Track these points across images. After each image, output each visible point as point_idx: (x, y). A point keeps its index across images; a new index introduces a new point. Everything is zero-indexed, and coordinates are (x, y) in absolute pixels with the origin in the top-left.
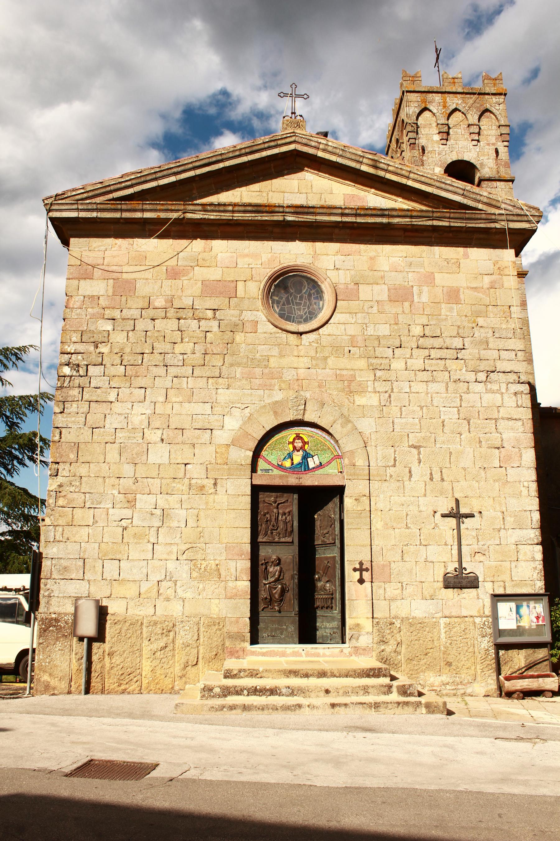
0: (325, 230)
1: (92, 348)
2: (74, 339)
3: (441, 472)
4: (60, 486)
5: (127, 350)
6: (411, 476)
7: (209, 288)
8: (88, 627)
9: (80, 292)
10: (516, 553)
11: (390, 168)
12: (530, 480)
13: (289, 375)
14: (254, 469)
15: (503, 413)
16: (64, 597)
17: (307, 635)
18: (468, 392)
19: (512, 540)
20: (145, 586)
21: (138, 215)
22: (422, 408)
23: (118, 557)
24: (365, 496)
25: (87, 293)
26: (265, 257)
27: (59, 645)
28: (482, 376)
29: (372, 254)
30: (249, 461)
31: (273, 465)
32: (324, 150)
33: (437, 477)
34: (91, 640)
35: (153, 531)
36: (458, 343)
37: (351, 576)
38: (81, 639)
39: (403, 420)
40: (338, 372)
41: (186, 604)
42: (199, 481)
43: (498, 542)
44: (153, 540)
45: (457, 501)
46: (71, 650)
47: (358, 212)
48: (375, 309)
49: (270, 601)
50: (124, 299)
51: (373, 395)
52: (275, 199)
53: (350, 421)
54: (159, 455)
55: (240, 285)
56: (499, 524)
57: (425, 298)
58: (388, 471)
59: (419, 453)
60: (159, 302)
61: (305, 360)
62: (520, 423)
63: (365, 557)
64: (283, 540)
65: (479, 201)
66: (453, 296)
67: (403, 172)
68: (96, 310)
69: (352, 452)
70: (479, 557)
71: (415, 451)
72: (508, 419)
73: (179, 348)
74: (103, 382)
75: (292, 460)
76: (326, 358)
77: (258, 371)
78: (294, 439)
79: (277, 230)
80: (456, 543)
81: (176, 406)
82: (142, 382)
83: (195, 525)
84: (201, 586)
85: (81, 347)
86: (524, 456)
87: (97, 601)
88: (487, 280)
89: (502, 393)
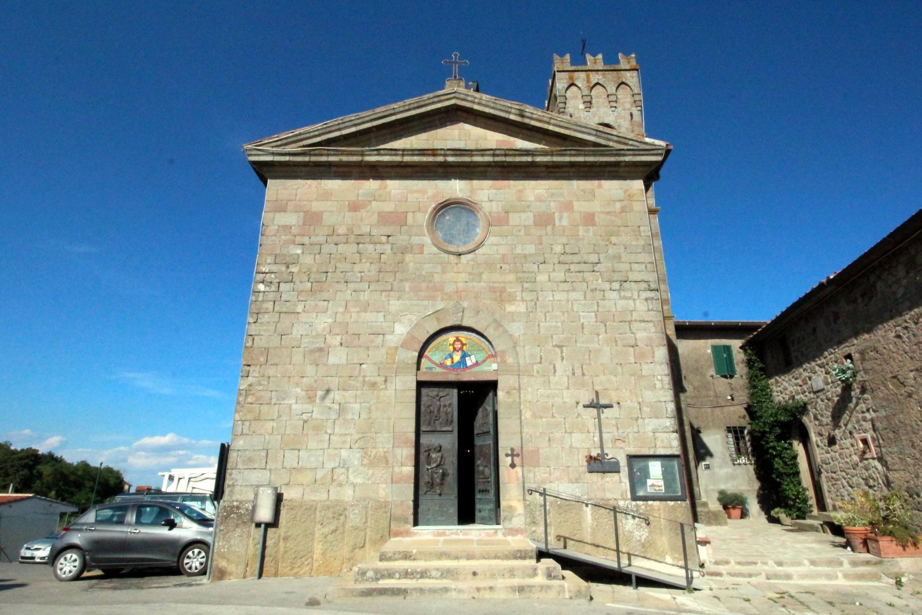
0: (479, 169)
1: (284, 268)
2: (269, 261)
4: (250, 385)
5: (315, 269)
6: (555, 371)
7: (384, 218)
8: (265, 514)
9: (275, 222)
11: (534, 116)
13: (450, 288)
14: (418, 369)
15: (635, 316)
16: (246, 486)
17: (466, 516)
18: (604, 299)
19: (649, 428)
20: (320, 474)
21: (324, 159)
22: (563, 313)
23: (298, 447)
25: (281, 224)
26: (430, 192)
27: (238, 530)
28: (616, 285)
29: (521, 187)
30: (415, 360)
31: (436, 364)
32: (479, 104)
33: (578, 372)
34: (268, 525)
35: (330, 423)
36: (593, 258)
37: (505, 461)
38: (258, 525)
39: (548, 324)
40: (491, 285)
41: (357, 489)
42: (372, 379)
43: (636, 430)
44: (329, 431)
45: (597, 393)
46: (249, 536)
48: (522, 233)
49: (431, 485)
50: (312, 228)
51: (521, 303)
52: (438, 145)
53: (501, 326)
54: (338, 357)
55: (410, 216)
56: (636, 413)
57: (565, 222)
58: (535, 367)
59: (562, 352)
60: (342, 230)
61: (463, 275)
62: (651, 324)
63: (515, 443)
64: (444, 429)
65: (610, 140)
66: (589, 219)
67: (545, 119)
68: (289, 237)
69: (503, 352)
70: (618, 443)
71: (558, 350)
72: (640, 321)
73: (357, 268)
74: (292, 296)
75: (452, 359)
76: (481, 274)
77: (424, 285)
78: (455, 342)
79: (440, 170)
80: (598, 431)
81: (354, 315)
82: (325, 295)
83: (367, 417)
84: (370, 472)
85: (274, 268)
86: (657, 354)
87: (276, 489)
88: (618, 205)
89: (634, 300)
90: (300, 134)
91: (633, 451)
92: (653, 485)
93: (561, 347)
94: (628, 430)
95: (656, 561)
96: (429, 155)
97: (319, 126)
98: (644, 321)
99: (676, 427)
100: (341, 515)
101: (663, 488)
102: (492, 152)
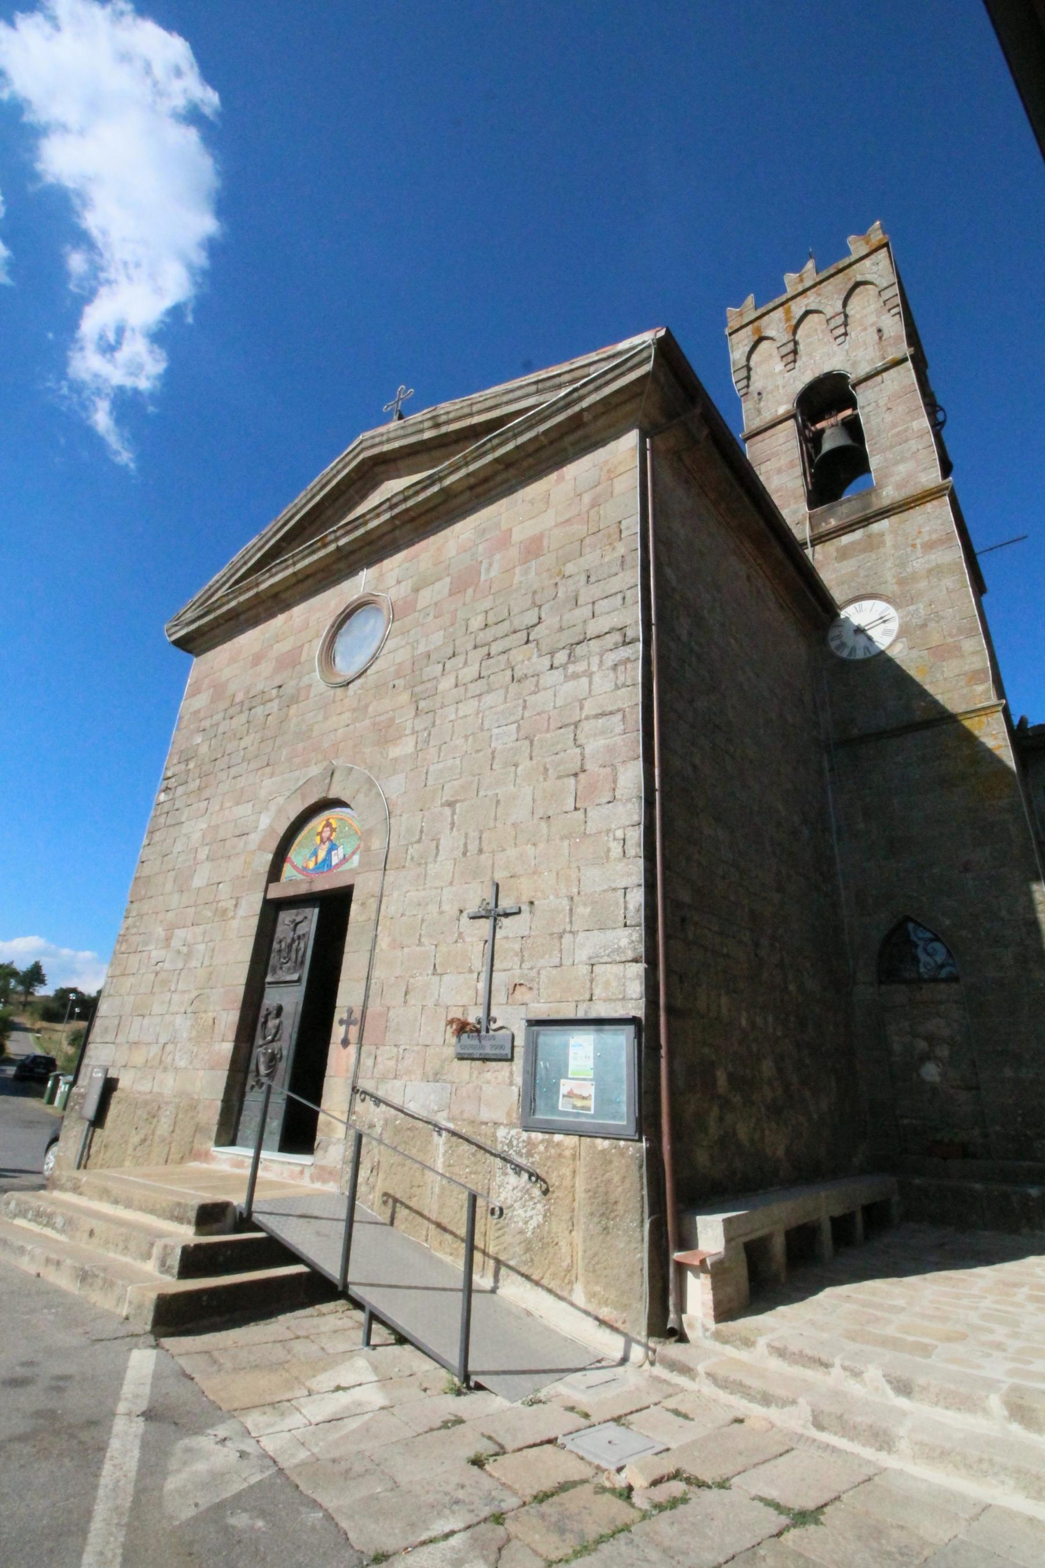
3: (480, 838)
6: (437, 855)
10: (588, 984)
12: (627, 823)
19: (583, 955)
24: (373, 896)
33: (473, 848)
47: (406, 494)
71: (447, 811)
76: (367, 706)
86: (622, 782)
90: (211, 587)
91: (542, 1010)
92: (570, 1095)
93: (451, 804)
94: (542, 962)
95: (550, 1291)
96: (319, 549)
97: (225, 570)
98: (603, 714)
99: (641, 949)
100: (154, 1117)
101: (591, 1103)
102: (387, 504)
